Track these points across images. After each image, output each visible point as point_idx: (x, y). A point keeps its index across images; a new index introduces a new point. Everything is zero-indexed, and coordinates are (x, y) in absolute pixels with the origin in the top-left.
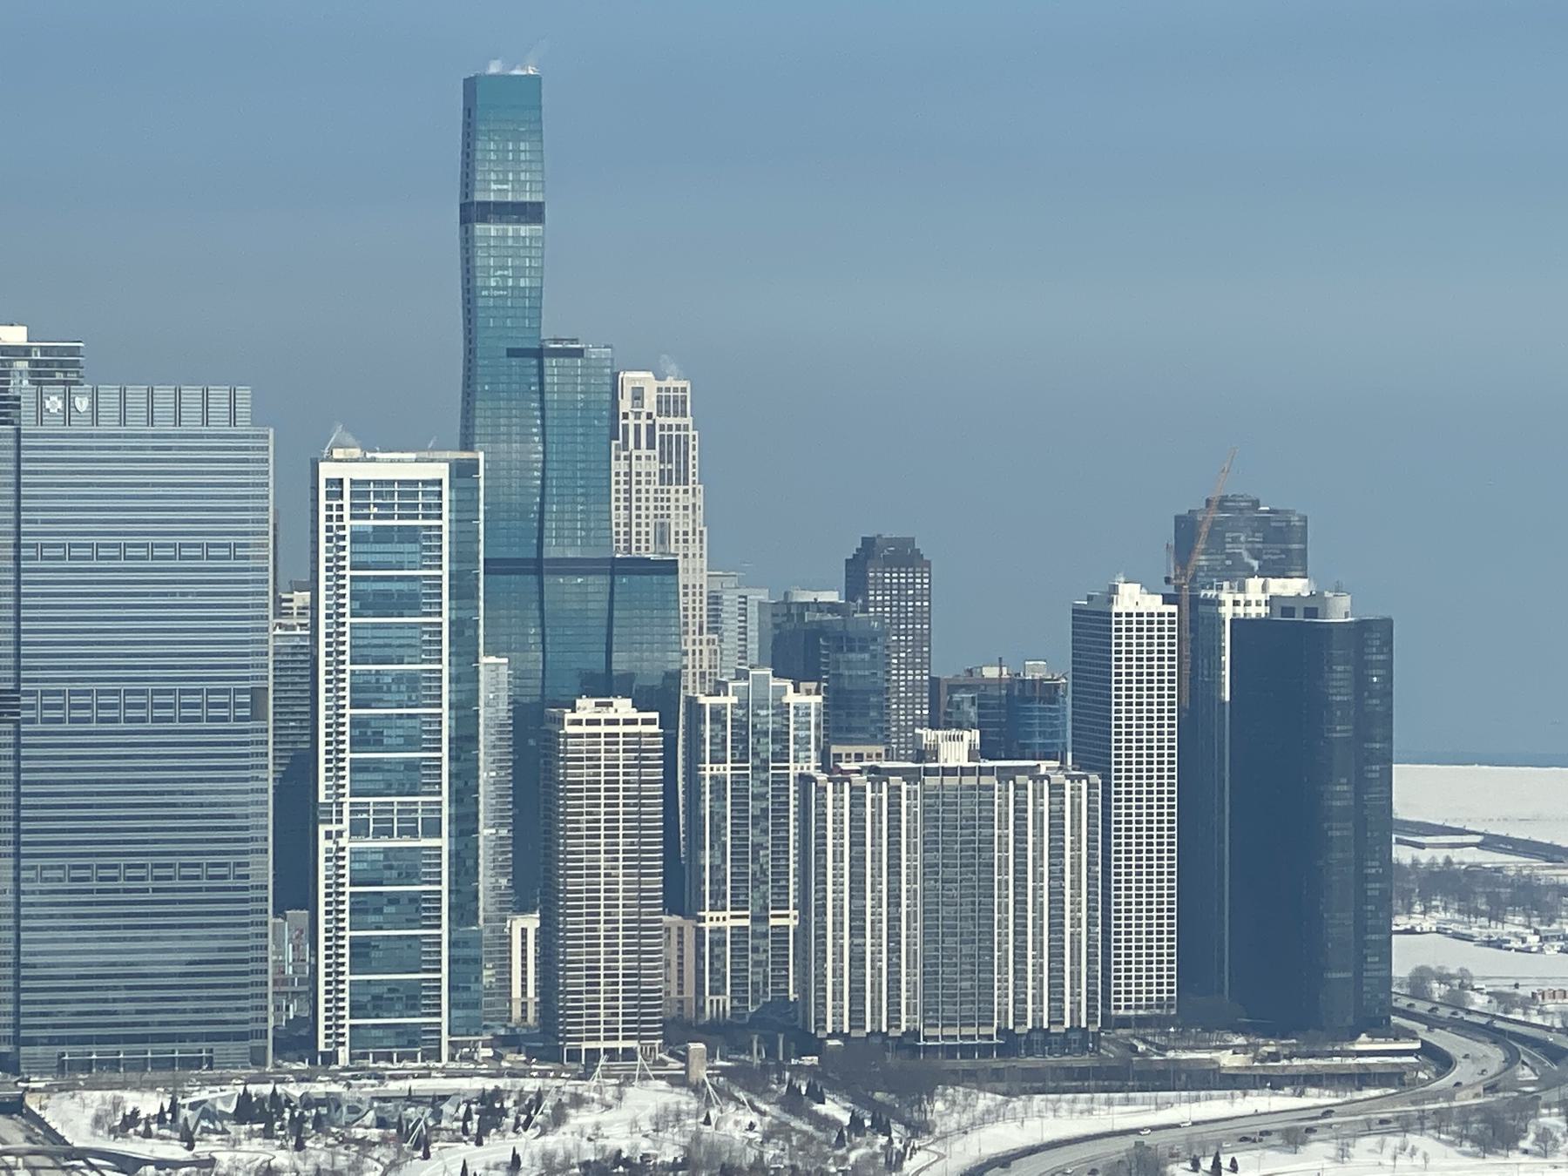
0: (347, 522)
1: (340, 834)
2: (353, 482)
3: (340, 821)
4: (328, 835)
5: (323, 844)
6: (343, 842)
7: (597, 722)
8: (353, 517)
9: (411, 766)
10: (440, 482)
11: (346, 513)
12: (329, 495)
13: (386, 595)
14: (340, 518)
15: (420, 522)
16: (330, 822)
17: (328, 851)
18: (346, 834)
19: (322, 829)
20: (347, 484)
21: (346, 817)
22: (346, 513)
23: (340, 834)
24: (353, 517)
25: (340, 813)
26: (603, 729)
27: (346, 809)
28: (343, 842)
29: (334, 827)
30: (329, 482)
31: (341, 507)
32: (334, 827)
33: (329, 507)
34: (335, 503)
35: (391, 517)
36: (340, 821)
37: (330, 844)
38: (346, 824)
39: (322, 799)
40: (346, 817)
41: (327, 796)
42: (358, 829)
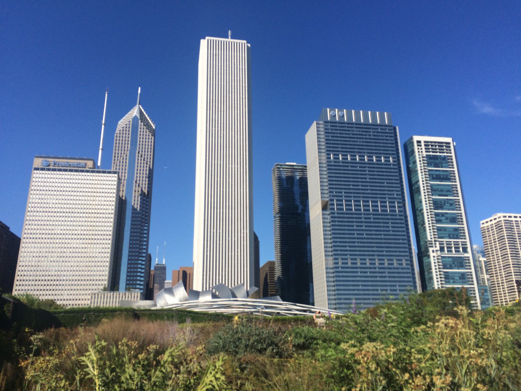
2: (425, 142)
4: (433, 251)
8: (426, 152)
9: (456, 229)
10: (449, 143)
12: (418, 145)
13: (440, 175)
14: (422, 152)
15: (445, 154)
16: (432, 247)
17: (434, 257)
19: (431, 249)
22: (424, 150)
23: (437, 251)
24: (426, 152)
27: (437, 243)
31: (421, 149)
32: (434, 249)
33: (418, 149)
34: (420, 147)
35: (437, 152)
36: (436, 247)
37: (435, 254)
38: (438, 248)
39: (429, 239)
41: (431, 238)
42: (442, 249)
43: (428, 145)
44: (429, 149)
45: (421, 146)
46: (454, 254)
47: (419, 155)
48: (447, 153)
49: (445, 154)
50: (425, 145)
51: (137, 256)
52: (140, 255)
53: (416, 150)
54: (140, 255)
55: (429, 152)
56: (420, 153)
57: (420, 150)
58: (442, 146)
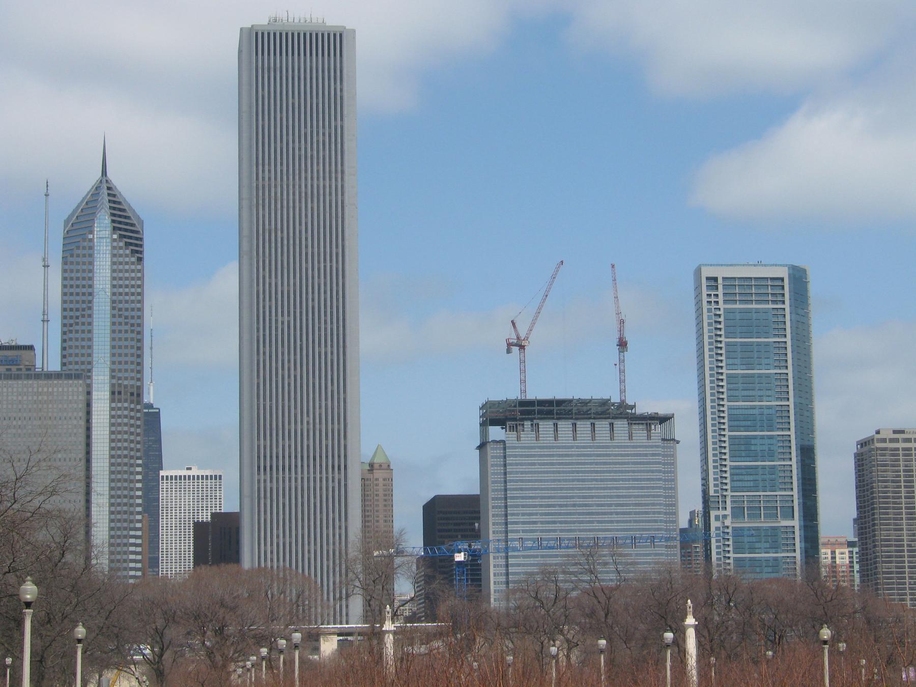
0: (721, 305)
1: (725, 517)
5: (714, 524)
6: (728, 522)
7: (897, 440)
8: (725, 302)
10: (782, 279)
11: (721, 299)
14: (717, 303)
17: (717, 529)
18: (729, 518)
19: (713, 514)
20: (720, 281)
21: (729, 505)
22: (721, 299)
23: (725, 517)
26: (901, 445)
27: (728, 500)
28: (728, 522)
29: (721, 513)
30: (708, 279)
31: (717, 296)
32: (721, 513)
34: (713, 293)
37: (719, 524)
38: (728, 512)
40: (729, 505)
41: (716, 491)
42: (738, 512)
46: (764, 523)
47: (709, 310)
49: (771, 306)
51: (125, 529)
52: (132, 525)
54: (132, 525)
56: (713, 306)
57: (713, 299)
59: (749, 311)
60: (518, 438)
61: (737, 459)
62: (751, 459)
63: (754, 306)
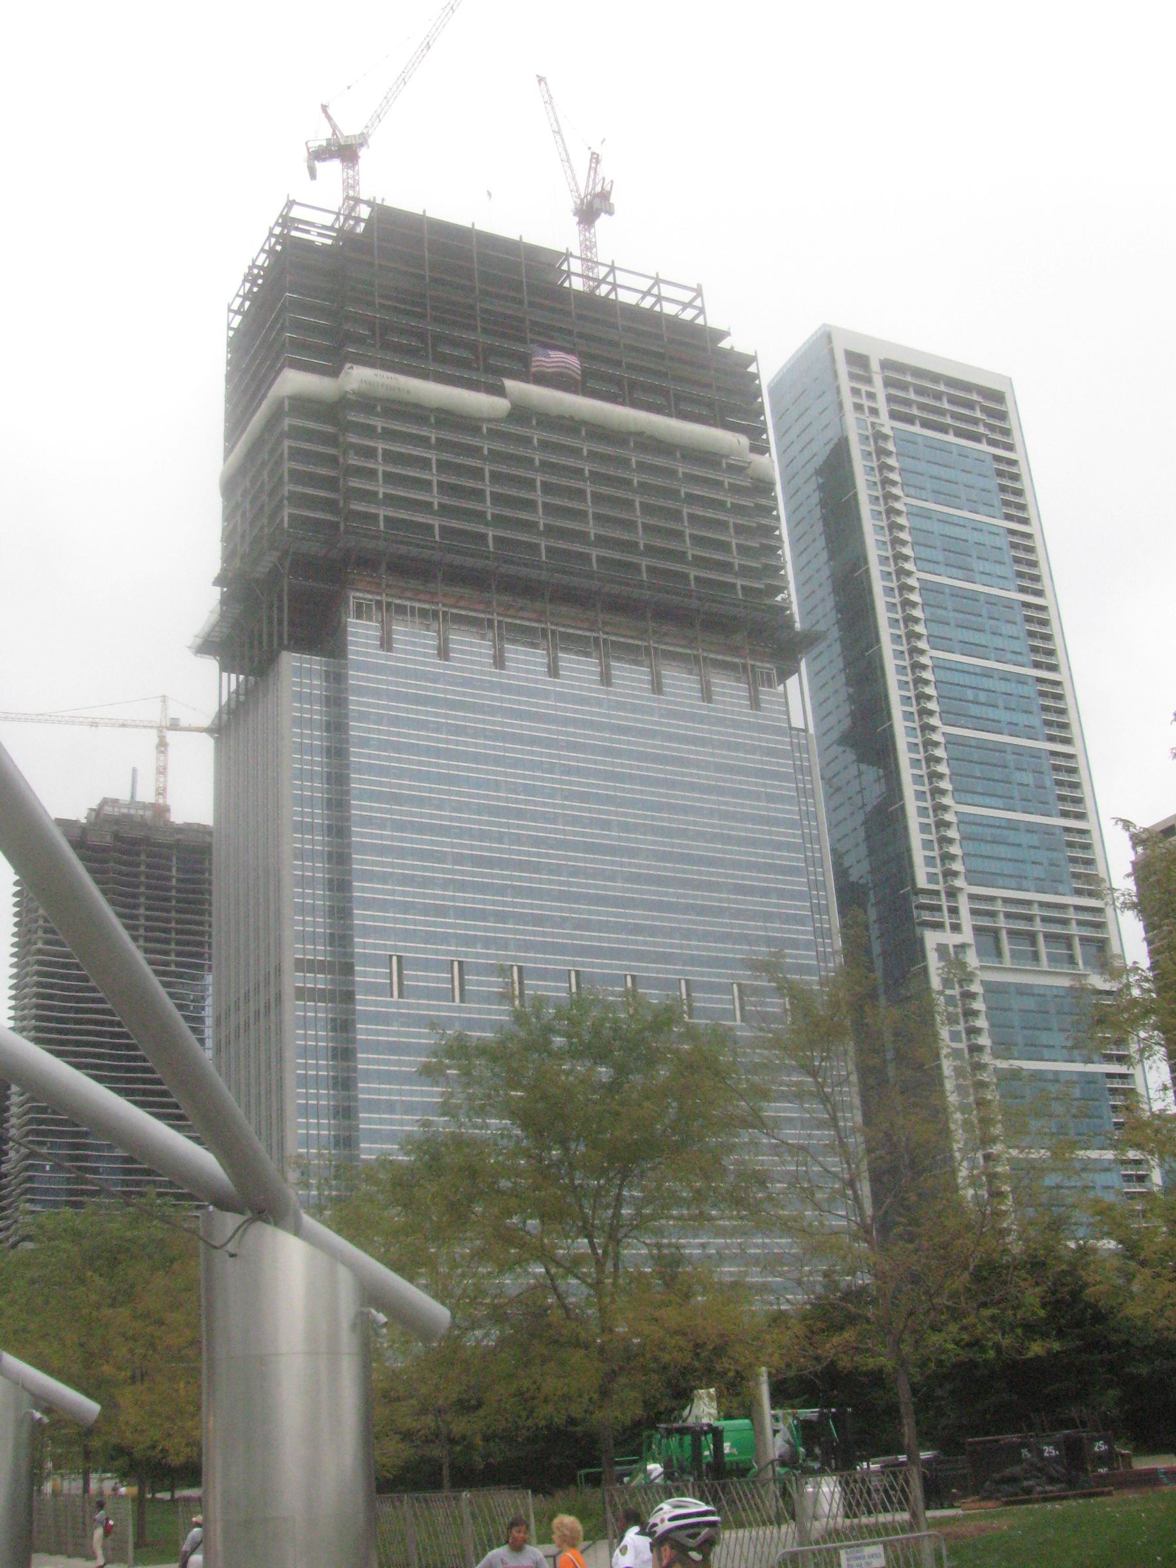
2: (886, 365)
3: (956, 928)
12: (852, 376)
16: (938, 926)
20: (875, 366)
23: (962, 947)
24: (894, 415)
25: (954, 911)
31: (871, 396)
32: (950, 939)
33: (856, 392)
34: (864, 388)
36: (956, 928)
38: (967, 936)
39: (922, 882)
41: (932, 878)
43: (904, 386)
44: (907, 403)
45: (869, 381)
48: (993, 443)
49: (984, 447)
50: (888, 383)
53: (848, 400)
55: (910, 420)
58: (970, 405)
59: (944, 448)
60: (386, 643)
61: (970, 798)
62: (1000, 802)
63: (950, 438)
